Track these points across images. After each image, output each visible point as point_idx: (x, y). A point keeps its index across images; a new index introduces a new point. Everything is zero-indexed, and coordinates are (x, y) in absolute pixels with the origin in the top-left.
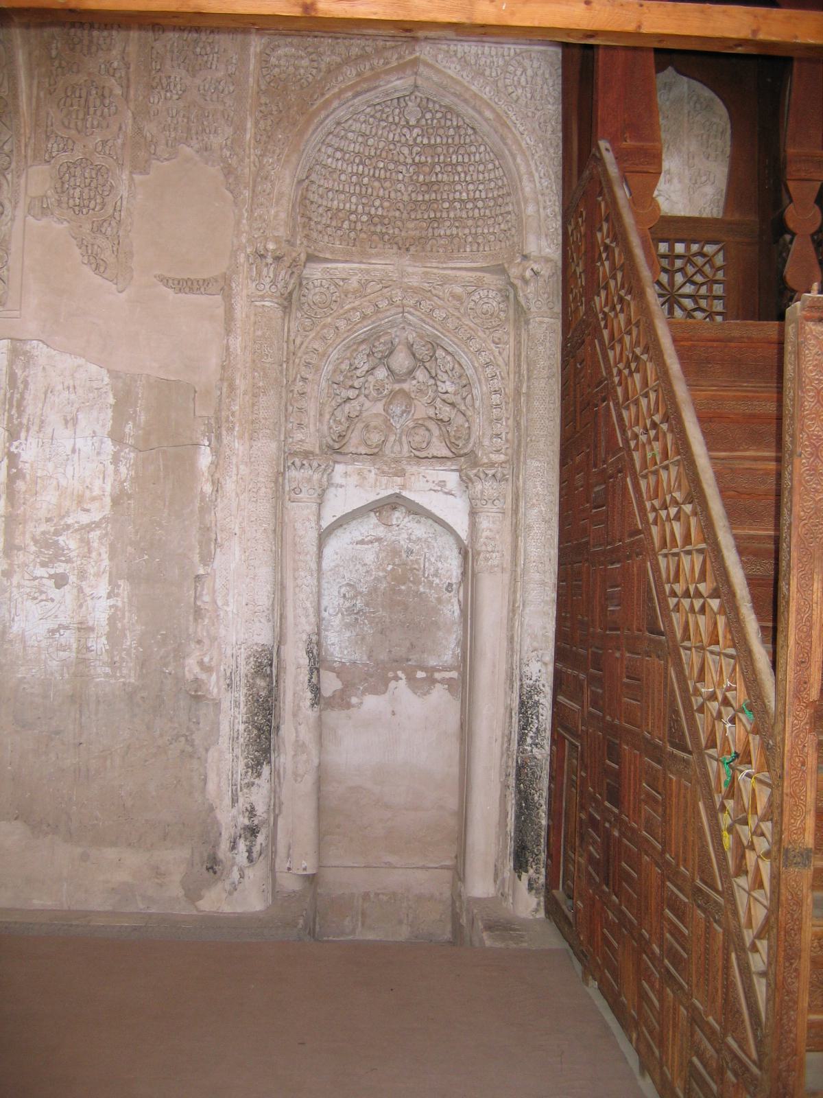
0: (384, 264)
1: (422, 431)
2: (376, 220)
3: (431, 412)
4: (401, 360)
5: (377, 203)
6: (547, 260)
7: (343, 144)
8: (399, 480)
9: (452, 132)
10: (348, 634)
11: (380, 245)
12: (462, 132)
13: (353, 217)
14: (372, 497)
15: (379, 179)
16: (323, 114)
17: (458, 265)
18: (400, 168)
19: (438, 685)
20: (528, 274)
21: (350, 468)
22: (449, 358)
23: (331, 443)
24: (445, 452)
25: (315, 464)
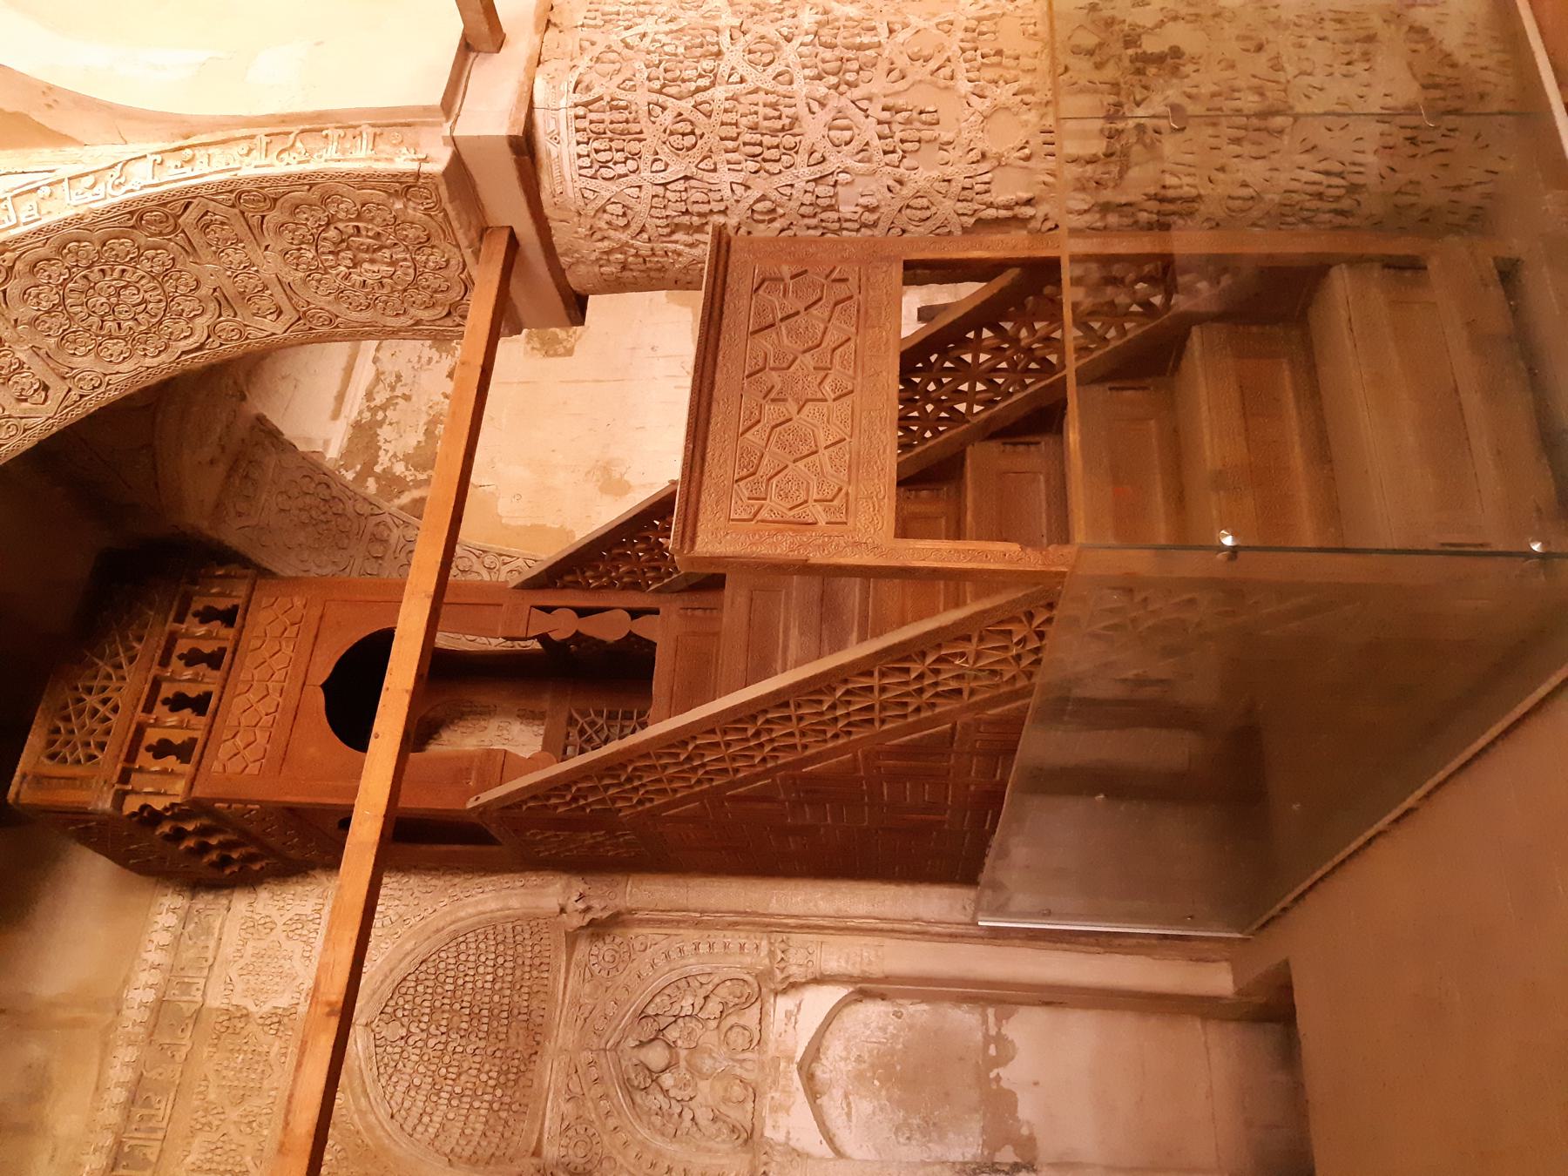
0: (551, 1073)
1: (732, 1035)
2: (502, 1079)
3: (713, 1024)
4: (656, 1056)
5: (484, 1077)
6: (568, 886)
7: (415, 1112)
8: (783, 1064)
9: (420, 988)
10: (951, 1135)
11: (529, 1075)
12: (422, 976)
13: (496, 1106)
14: (801, 1098)
15: (459, 1075)
16: (379, 1132)
17: (561, 986)
18: (450, 1048)
19: (1003, 1031)
20: (581, 906)
21: (769, 1123)
22: (658, 1000)
23: (741, 1141)
24: (756, 1008)
25: (764, 1158)
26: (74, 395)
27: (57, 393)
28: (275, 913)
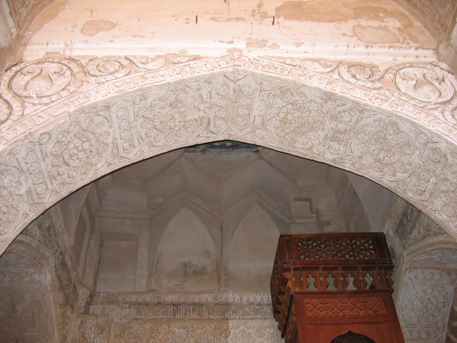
26: (425, 203)
27: (423, 197)
28: (266, 336)
